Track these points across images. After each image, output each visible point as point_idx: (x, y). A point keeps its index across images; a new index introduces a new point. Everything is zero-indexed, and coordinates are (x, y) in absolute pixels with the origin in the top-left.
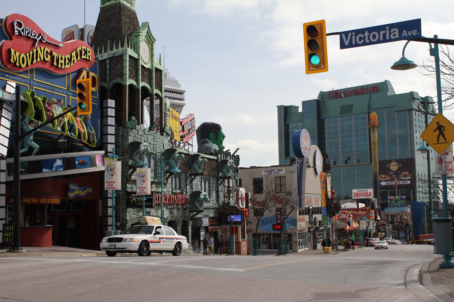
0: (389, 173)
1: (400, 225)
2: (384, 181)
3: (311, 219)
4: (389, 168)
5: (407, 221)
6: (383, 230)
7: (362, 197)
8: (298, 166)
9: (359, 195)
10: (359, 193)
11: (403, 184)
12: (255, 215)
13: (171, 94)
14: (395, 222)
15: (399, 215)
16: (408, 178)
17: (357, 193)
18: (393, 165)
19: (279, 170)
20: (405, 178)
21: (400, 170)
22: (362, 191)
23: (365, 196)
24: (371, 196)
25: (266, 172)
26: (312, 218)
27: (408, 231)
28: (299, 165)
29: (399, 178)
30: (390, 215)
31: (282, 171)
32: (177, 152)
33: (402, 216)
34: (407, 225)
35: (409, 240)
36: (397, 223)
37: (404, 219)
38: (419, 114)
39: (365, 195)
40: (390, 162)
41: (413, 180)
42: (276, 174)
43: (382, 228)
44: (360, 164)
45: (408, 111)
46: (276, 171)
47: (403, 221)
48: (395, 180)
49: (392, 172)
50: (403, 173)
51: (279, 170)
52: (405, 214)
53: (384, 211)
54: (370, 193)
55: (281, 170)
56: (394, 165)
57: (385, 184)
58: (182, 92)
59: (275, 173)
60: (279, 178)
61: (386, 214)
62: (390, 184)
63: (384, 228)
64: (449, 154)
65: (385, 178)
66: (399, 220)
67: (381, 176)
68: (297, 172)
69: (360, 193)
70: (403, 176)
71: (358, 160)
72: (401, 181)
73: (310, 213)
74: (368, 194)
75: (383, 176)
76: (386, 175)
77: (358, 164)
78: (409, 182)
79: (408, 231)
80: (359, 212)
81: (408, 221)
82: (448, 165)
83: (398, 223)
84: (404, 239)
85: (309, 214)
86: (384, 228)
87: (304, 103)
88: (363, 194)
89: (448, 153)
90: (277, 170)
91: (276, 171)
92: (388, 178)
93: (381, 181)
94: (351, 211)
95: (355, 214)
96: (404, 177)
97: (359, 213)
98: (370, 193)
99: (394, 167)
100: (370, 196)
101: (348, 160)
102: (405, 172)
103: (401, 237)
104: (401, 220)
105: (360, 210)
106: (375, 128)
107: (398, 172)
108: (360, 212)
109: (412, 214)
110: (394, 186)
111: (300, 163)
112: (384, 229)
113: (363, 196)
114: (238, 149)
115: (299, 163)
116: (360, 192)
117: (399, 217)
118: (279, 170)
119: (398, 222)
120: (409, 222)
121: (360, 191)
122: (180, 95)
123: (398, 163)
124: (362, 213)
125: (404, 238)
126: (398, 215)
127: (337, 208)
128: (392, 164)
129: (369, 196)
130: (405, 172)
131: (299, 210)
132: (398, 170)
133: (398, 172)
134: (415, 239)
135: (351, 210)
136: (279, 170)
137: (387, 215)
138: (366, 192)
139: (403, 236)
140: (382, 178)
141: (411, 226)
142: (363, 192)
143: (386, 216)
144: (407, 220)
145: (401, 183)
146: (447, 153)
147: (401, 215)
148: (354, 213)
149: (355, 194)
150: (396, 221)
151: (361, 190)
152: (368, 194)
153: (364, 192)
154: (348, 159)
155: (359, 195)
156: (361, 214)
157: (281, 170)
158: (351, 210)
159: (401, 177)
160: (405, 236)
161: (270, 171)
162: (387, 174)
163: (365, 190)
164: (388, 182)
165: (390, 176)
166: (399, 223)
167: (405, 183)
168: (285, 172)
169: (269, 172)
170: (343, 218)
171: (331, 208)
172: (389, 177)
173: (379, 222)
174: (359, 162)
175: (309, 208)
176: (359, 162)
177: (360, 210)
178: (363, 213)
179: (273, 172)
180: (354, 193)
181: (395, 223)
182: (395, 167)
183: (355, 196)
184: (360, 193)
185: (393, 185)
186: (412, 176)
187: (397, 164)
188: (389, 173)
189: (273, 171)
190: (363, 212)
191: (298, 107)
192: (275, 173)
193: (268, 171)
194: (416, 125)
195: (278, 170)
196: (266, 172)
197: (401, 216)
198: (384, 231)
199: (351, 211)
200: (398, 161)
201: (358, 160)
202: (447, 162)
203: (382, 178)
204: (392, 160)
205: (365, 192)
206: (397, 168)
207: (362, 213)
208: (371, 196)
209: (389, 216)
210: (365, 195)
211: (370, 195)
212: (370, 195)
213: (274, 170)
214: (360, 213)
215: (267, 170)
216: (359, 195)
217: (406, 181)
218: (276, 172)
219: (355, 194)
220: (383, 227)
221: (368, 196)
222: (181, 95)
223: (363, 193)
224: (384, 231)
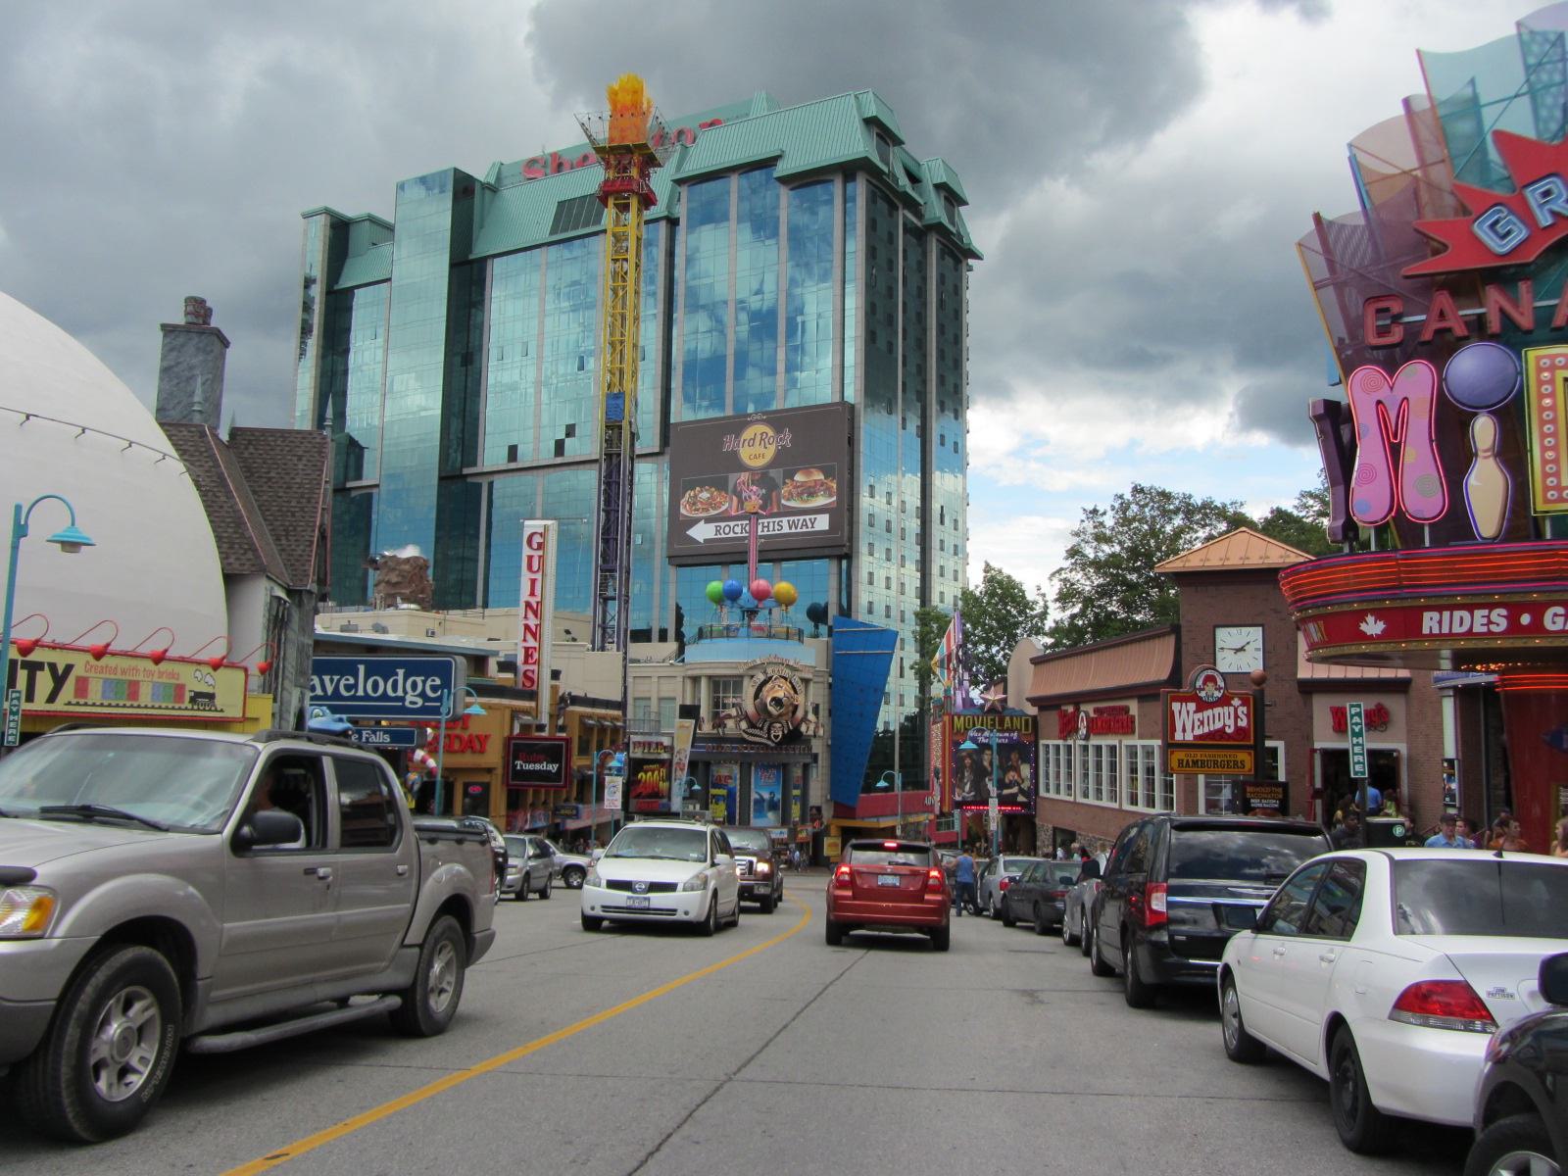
0: (733, 478)
1: (757, 732)
2: (708, 520)
4: (735, 455)
5: (794, 712)
11: (793, 530)
12: (190, 702)
14: (729, 717)
16: (821, 501)
18: (754, 440)
20: (803, 501)
27: (798, 772)
29: (779, 501)
30: (710, 677)
34: (794, 737)
35: (803, 820)
36: (737, 724)
37: (777, 701)
41: (846, 512)
45: (837, 187)
47: (769, 714)
49: (744, 476)
50: (799, 477)
52: (787, 672)
56: (758, 438)
57: (711, 535)
60: (617, 697)
61: (690, 673)
62: (731, 535)
65: (711, 504)
67: (695, 496)
70: (794, 491)
72: (785, 520)
75: (705, 495)
76: (718, 489)
78: (822, 523)
79: (798, 772)
81: (800, 714)
83: (744, 725)
84: (771, 815)
92: (727, 505)
93: (694, 522)
96: (800, 495)
99: (757, 448)
101: (567, 440)
102: (807, 471)
103: (760, 802)
104: (762, 709)
109: (830, 686)
119: (747, 717)
120: (805, 719)
123: (778, 430)
125: (773, 806)
126: (746, 682)
128: (748, 434)
130: (808, 474)
132: (774, 463)
133: (773, 473)
134: (836, 816)
137: (696, 680)
139: (766, 796)
140: (699, 506)
141: (817, 746)
143: (689, 683)
144: (796, 707)
145: (785, 526)
147: (762, 677)
150: (733, 712)
154: (568, 435)
159: (788, 500)
160: (778, 796)
162: (721, 485)
164: (723, 524)
166: (752, 725)
167: (804, 529)
172: (731, 500)
181: (730, 723)
182: (762, 450)
188: (733, 478)
194: (942, 437)
197: (765, 683)
200: (778, 421)
206: (770, 452)
209: (704, 683)
217: (807, 517)
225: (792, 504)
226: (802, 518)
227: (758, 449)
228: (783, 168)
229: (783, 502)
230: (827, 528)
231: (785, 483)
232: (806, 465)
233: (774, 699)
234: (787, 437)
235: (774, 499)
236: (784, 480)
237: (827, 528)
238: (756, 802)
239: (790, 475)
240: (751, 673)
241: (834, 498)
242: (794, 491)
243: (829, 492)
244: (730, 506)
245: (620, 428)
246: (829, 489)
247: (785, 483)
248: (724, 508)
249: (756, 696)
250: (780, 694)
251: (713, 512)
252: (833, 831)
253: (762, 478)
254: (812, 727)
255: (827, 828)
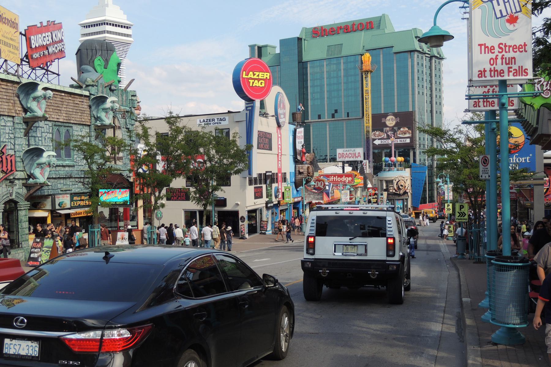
0: (385, 129)
2: (379, 139)
3: (269, 190)
4: (385, 123)
5: (405, 188)
6: (375, 200)
7: (349, 158)
8: (247, 114)
9: (346, 157)
10: (345, 153)
11: (401, 142)
13: (114, 27)
14: (391, 189)
15: (395, 180)
16: (407, 135)
17: (342, 154)
19: (221, 119)
21: (398, 125)
22: (349, 151)
23: (352, 157)
24: (360, 157)
25: (203, 122)
26: (271, 189)
28: (248, 112)
29: (397, 135)
30: (385, 180)
31: (225, 120)
32: (40, 88)
33: (399, 182)
34: (405, 193)
37: (402, 186)
38: (422, 57)
39: (353, 156)
40: (385, 115)
42: (216, 124)
43: (373, 198)
44: (350, 118)
46: (216, 121)
47: (400, 189)
48: (391, 137)
49: (388, 129)
50: (402, 129)
51: (221, 120)
52: (403, 179)
53: (377, 175)
54: (359, 153)
55: (224, 119)
56: (391, 119)
58: (129, 26)
59: (215, 123)
62: (385, 143)
63: (376, 198)
64: (518, 21)
66: (396, 188)
67: (375, 133)
68: (245, 122)
69: (347, 154)
70: (401, 133)
71: (348, 113)
72: (399, 140)
73: (268, 182)
74: (357, 155)
75: (377, 133)
77: (348, 118)
78: (408, 141)
80: (342, 178)
81: (406, 188)
82: (514, 58)
85: (265, 183)
86: (376, 198)
87: (283, 42)
88: (350, 155)
89: (517, 18)
90: (218, 119)
91: (216, 121)
92: (383, 136)
93: (374, 140)
94: (332, 177)
95: (338, 181)
96: (402, 134)
97: (343, 179)
98: (359, 153)
99: (390, 121)
100: (359, 157)
105: (344, 176)
106: (368, 73)
107: (396, 128)
108: (344, 178)
109: (411, 179)
110: (391, 145)
111: (250, 108)
112: (376, 199)
113: (350, 158)
114: (133, 80)
115: (248, 108)
116: (346, 152)
117: (395, 184)
118: (221, 120)
121: (346, 151)
122: (126, 29)
123: (396, 117)
124: (346, 179)
125: (401, 209)
126: (394, 181)
127: (309, 173)
128: (388, 118)
129: (357, 157)
131: (249, 178)
132: (395, 126)
133: (395, 128)
135: (333, 175)
136: (221, 119)
137: (381, 181)
138: (354, 152)
139: (399, 206)
140: (376, 136)
141: (409, 194)
142: (350, 152)
143: (379, 182)
144: (405, 186)
145: (399, 141)
146: (511, 16)
147: (398, 180)
148: (336, 179)
149: (340, 155)
151: (347, 149)
152: (357, 155)
153: (351, 152)
155: (345, 156)
156: (345, 181)
157: (224, 119)
158: (333, 175)
160: (402, 206)
161: (208, 121)
163: (353, 149)
164: (383, 140)
165: (385, 132)
168: (229, 122)
169: (207, 122)
170: (318, 187)
171: (300, 173)
173: (369, 191)
174: (348, 116)
175: (266, 174)
176: (348, 116)
177: (344, 176)
178: (347, 180)
179: (212, 123)
180: (339, 154)
182: (392, 122)
183: (340, 158)
184: (347, 154)
185: (390, 144)
186: (412, 134)
187: (394, 118)
188: (385, 129)
189: (212, 120)
190: (347, 178)
191: (275, 47)
192: (215, 123)
193: (206, 121)
195: (219, 120)
196: (203, 122)
197: (398, 181)
198: (375, 201)
199: (332, 177)
200: (396, 115)
201: (348, 113)
202: (510, 46)
203: (376, 136)
204: (389, 113)
205: (353, 152)
206: (394, 123)
207: (346, 179)
208: (360, 157)
209: (384, 181)
210: (353, 156)
211: (358, 156)
212: (358, 156)
213: (214, 119)
214: (344, 180)
215: (204, 120)
216: (346, 157)
217: (404, 139)
218: (217, 122)
219: (340, 155)
220: (374, 197)
221: (356, 157)
222: (127, 30)
223: (350, 153)
224: (375, 201)
225: (400, 136)
226: (403, 139)
227: (391, 122)
228: (395, 50)
229: (398, 135)
230: (409, 142)
231: (398, 131)
232: (404, 126)
233: (401, 185)
234: (398, 119)
235: (396, 135)
236: (398, 130)
237: (409, 142)
238: (397, 207)
239: (399, 129)
240: (395, 179)
241: (411, 135)
242: (401, 133)
243: (409, 133)
244: (384, 136)
245: (369, 132)
246: (409, 132)
247: (398, 131)
248: (382, 136)
249: (397, 185)
250: (402, 184)
251: (380, 137)
252: (413, 213)
253: (392, 129)
254: (409, 190)
255: (412, 212)
